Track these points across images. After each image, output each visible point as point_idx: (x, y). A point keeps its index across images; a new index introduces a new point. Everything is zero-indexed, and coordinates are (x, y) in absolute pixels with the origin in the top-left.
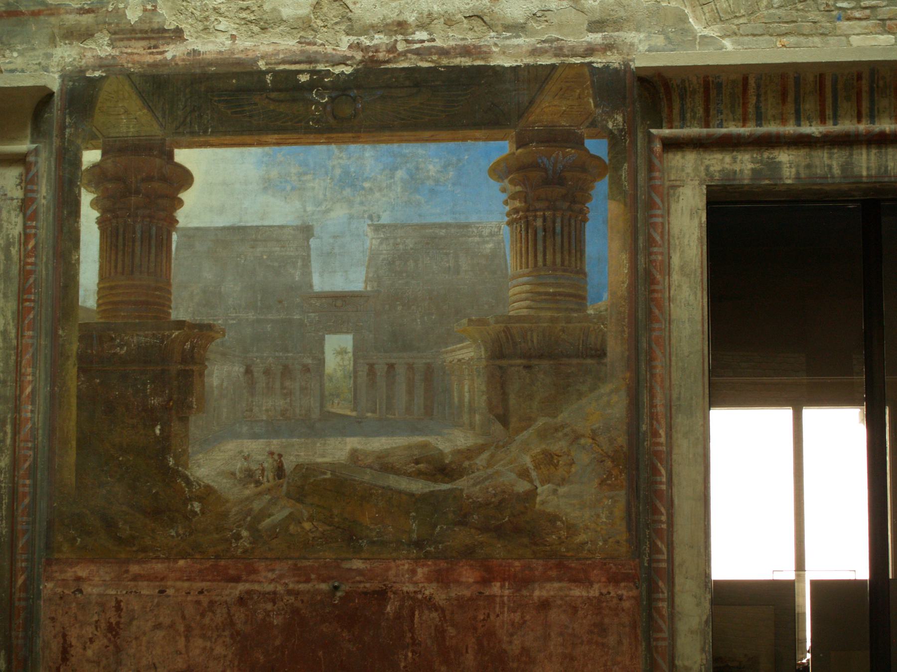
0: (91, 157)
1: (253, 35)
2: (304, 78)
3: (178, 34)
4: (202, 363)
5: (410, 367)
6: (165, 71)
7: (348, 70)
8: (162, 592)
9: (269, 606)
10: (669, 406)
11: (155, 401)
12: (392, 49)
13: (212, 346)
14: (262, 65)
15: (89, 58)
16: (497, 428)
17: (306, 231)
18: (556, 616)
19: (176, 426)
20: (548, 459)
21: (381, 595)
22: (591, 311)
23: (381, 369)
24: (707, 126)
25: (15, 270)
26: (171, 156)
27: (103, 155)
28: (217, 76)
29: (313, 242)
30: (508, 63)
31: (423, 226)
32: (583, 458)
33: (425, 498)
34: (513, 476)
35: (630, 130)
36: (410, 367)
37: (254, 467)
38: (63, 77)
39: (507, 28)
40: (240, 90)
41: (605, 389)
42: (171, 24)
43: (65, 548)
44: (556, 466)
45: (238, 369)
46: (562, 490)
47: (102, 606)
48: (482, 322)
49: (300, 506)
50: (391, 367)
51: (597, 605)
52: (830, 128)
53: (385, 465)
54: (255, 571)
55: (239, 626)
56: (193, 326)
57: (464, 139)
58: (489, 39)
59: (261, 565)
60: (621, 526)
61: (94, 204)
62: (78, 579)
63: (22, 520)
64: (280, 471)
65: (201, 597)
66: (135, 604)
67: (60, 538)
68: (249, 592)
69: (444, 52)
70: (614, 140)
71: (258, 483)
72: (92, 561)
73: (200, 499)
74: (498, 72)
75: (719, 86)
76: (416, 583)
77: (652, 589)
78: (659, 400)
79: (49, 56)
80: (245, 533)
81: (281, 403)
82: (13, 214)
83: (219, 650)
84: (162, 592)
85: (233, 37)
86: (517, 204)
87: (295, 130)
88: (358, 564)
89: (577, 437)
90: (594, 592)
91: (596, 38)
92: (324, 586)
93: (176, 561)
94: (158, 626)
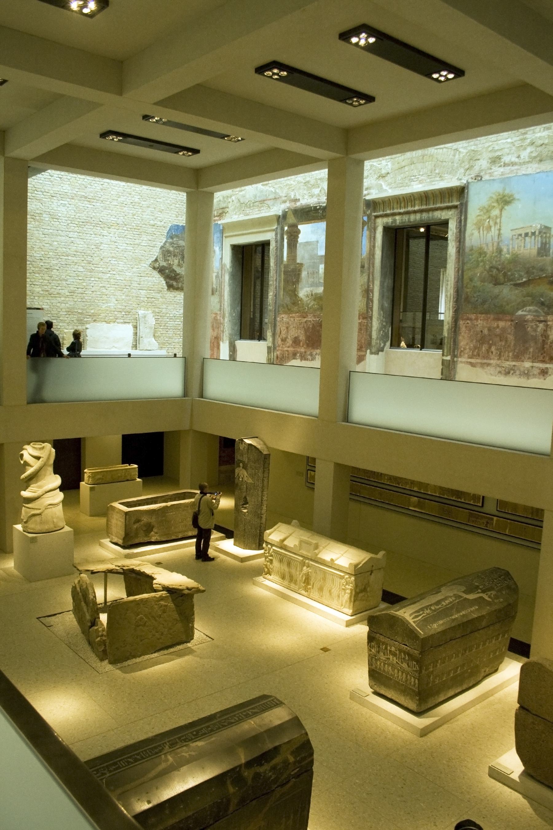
2: (318, 207)
6: (297, 208)
13: (303, 268)
14: (312, 205)
15: (286, 207)
17: (317, 242)
40: (309, 211)
42: (298, 198)
45: (307, 273)
52: (406, 210)
54: (307, 316)
59: (308, 315)
64: (312, 295)
68: (307, 320)
73: (300, 301)
79: (280, 207)
81: (313, 280)
83: (302, 332)
92: (318, 319)
94: (294, 327)
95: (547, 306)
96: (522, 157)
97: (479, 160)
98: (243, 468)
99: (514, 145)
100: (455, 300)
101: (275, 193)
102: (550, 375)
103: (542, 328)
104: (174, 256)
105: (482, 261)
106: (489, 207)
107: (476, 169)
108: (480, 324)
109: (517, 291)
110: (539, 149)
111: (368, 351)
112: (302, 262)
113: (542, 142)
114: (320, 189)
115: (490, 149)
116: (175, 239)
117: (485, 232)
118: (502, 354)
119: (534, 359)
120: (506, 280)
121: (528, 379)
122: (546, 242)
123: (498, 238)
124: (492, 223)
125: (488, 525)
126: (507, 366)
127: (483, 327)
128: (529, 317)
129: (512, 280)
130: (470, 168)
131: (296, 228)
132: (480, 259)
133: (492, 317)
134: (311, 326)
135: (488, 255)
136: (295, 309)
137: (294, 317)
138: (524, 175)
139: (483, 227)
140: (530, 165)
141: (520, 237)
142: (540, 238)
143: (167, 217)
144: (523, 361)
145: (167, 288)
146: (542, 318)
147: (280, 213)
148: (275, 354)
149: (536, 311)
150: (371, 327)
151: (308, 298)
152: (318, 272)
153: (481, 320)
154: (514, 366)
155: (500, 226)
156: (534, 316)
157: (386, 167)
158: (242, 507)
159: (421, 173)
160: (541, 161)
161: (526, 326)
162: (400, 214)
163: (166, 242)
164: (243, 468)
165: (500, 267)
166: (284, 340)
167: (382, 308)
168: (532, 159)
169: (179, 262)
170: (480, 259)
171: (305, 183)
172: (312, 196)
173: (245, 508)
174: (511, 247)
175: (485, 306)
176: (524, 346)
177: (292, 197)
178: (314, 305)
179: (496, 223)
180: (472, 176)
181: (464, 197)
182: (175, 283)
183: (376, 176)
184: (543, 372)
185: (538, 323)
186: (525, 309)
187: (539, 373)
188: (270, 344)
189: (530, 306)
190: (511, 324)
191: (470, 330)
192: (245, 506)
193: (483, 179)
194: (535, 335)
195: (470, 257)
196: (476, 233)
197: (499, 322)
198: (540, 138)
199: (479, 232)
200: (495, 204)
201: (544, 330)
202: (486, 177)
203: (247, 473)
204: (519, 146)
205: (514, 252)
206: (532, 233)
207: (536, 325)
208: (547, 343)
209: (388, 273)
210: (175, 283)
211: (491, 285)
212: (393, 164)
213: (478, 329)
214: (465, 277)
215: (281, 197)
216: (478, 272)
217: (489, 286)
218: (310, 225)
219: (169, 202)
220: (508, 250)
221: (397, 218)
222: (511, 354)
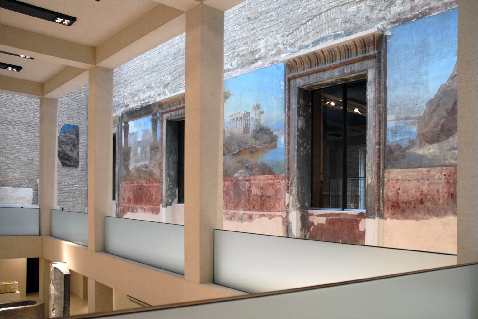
26: (128, 123)
31: (145, 130)
40: (133, 112)
48: (149, 144)
69: (147, 103)
95: (250, 169)
99: (229, 57)
101: (118, 101)
102: (254, 219)
104: (67, 144)
109: (233, 160)
110: (242, 58)
111: (161, 205)
113: (242, 53)
116: (67, 134)
118: (228, 205)
119: (245, 208)
120: (228, 151)
121: (242, 222)
122: (247, 123)
126: (231, 214)
128: (241, 178)
138: (235, 77)
140: (237, 70)
143: (60, 119)
144: (239, 210)
145: (61, 165)
146: (248, 178)
147: (120, 115)
148: (120, 209)
149: (244, 173)
150: (162, 189)
152: (138, 153)
154: (234, 213)
156: (243, 177)
160: (243, 66)
162: (174, 110)
163: (60, 135)
166: (124, 199)
167: (168, 175)
169: (71, 149)
171: (131, 94)
176: (239, 199)
177: (125, 103)
182: (68, 163)
184: (250, 217)
185: (245, 182)
186: (238, 172)
187: (248, 218)
188: (117, 202)
189: (241, 169)
194: (244, 190)
198: (242, 51)
205: (231, 132)
206: (240, 117)
208: (251, 197)
209: (173, 151)
210: (68, 163)
212: (171, 77)
218: (134, 121)
219: (62, 109)
220: (228, 130)
221: (173, 113)
222: (232, 205)
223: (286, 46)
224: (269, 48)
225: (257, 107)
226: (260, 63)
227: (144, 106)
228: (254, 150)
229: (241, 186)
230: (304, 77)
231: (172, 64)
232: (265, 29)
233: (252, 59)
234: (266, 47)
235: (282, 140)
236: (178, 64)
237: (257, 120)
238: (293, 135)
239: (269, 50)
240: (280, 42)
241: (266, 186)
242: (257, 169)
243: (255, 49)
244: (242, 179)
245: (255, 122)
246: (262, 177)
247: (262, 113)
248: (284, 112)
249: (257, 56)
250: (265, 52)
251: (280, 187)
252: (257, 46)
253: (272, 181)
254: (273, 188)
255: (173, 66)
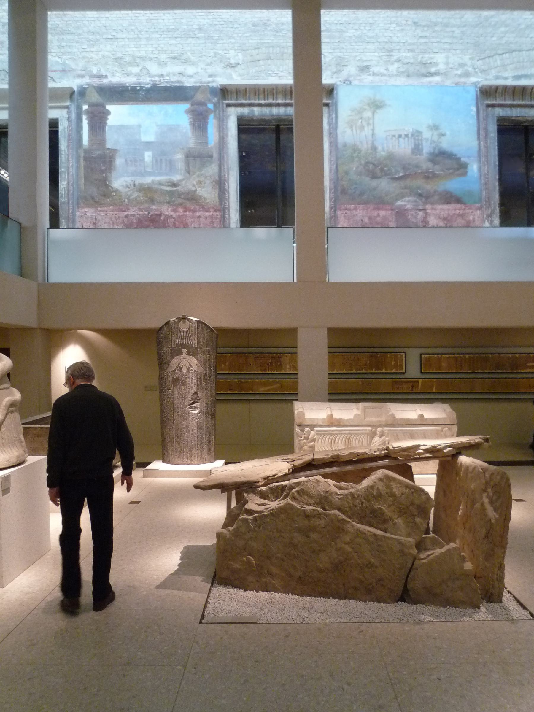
0: (85, 107)
1: (125, 77)
2: (138, 88)
3: (106, 77)
4: (114, 159)
5: (166, 160)
7: (149, 86)
8: (106, 214)
9: (133, 218)
10: (228, 169)
11: (103, 168)
12: (160, 81)
13: (117, 154)
14: (128, 85)
16: (187, 175)
17: (140, 126)
18: (202, 220)
19: (108, 174)
20: (200, 182)
21: (160, 215)
22: (209, 147)
23: (159, 160)
24: (237, 101)
25: (67, 135)
26: (105, 107)
27: (88, 107)
28: (116, 87)
29: (141, 129)
30: (188, 85)
32: (208, 182)
33: (170, 192)
34: (191, 186)
35: (218, 102)
36: (166, 160)
37: (128, 184)
38: (77, 87)
39: (189, 76)
40: (122, 91)
41: (213, 165)
43: (82, 204)
44: (201, 184)
45: (123, 160)
46: (203, 190)
47: (92, 218)
48: (183, 149)
49: (140, 193)
50: (161, 160)
51: (212, 217)
52: (266, 102)
53: (160, 184)
54: (129, 209)
55: (126, 222)
56: (112, 149)
57: (179, 104)
58: (184, 79)
59: (131, 208)
60: (217, 198)
61: (86, 119)
62: (85, 212)
63: (71, 196)
64: (134, 185)
65: (116, 216)
66: (100, 218)
67: (80, 202)
69: (172, 82)
70: (215, 105)
71: (129, 188)
72: (89, 207)
73: (115, 192)
74: (186, 88)
75: (240, 91)
76: (168, 212)
77: (224, 212)
78: (226, 167)
79: (73, 82)
80: (126, 200)
82: (66, 121)
84: (106, 214)
85: (120, 77)
86: (191, 120)
87: (136, 101)
88: (154, 207)
89: (206, 177)
90: (211, 214)
91: (210, 79)
92: (146, 213)
93: (109, 207)
96: (390, 70)
97: (346, 66)
98: (188, 354)
99: (381, 59)
100: (333, 191)
101: (64, 64)
103: (422, 216)
105: (357, 156)
106: (361, 109)
107: (344, 74)
108: (359, 213)
109: (395, 185)
110: (406, 66)
112: (114, 147)
113: (408, 61)
114: (140, 68)
115: (358, 58)
117: (358, 131)
120: (383, 174)
123: (372, 137)
124: (365, 124)
125: (414, 389)
127: (363, 216)
128: (409, 206)
129: (389, 174)
130: (339, 72)
131: (102, 109)
132: (355, 155)
133: (372, 206)
134: (135, 221)
135: (363, 152)
136: (109, 200)
137: (106, 211)
138: (393, 85)
139: (356, 128)
141: (394, 138)
142: (413, 141)
146: (421, 207)
149: (415, 201)
151: (127, 190)
152: (143, 160)
153: (360, 210)
155: (373, 127)
157: (237, 57)
158: (190, 408)
159: (281, 69)
160: (408, 76)
161: (407, 214)
164: (188, 354)
165: (376, 163)
168: (399, 74)
170: (355, 155)
171: (115, 59)
172: (128, 75)
173: (196, 408)
174: (385, 145)
175: (363, 198)
178: (138, 196)
179: (368, 124)
180: (340, 79)
181: (333, 98)
183: (223, 65)
185: (417, 211)
186: (404, 199)
189: (408, 197)
190: (391, 213)
191: (349, 219)
192: (194, 405)
193: (352, 83)
195: (344, 152)
196: (348, 131)
197: (380, 211)
198: (406, 57)
199: (352, 130)
200: (367, 107)
201: (424, 218)
202: (356, 82)
203: (197, 359)
204: (386, 61)
207: (416, 213)
211: (368, 179)
213: (358, 218)
214: (340, 171)
215: (74, 70)
216: (354, 167)
217: (367, 179)
220: (383, 148)
223: (476, 70)
224: (451, 66)
225: (435, 127)
226: (437, 79)
227: (163, 85)
228: (430, 176)
229: (409, 217)
230: (505, 108)
231: (247, 37)
232: (444, 43)
233: (424, 71)
234: (447, 63)
235: (474, 168)
236: (263, 41)
237: (434, 142)
238: (493, 165)
239: (452, 68)
240: (469, 63)
241: (452, 216)
242: (436, 197)
243: (429, 62)
244: (410, 208)
245: (431, 144)
246: (445, 207)
247: (444, 135)
248: (476, 139)
249: (433, 70)
250: (446, 69)
251: (474, 218)
252: (431, 58)
253: (461, 212)
254: (463, 219)
255: (250, 41)
